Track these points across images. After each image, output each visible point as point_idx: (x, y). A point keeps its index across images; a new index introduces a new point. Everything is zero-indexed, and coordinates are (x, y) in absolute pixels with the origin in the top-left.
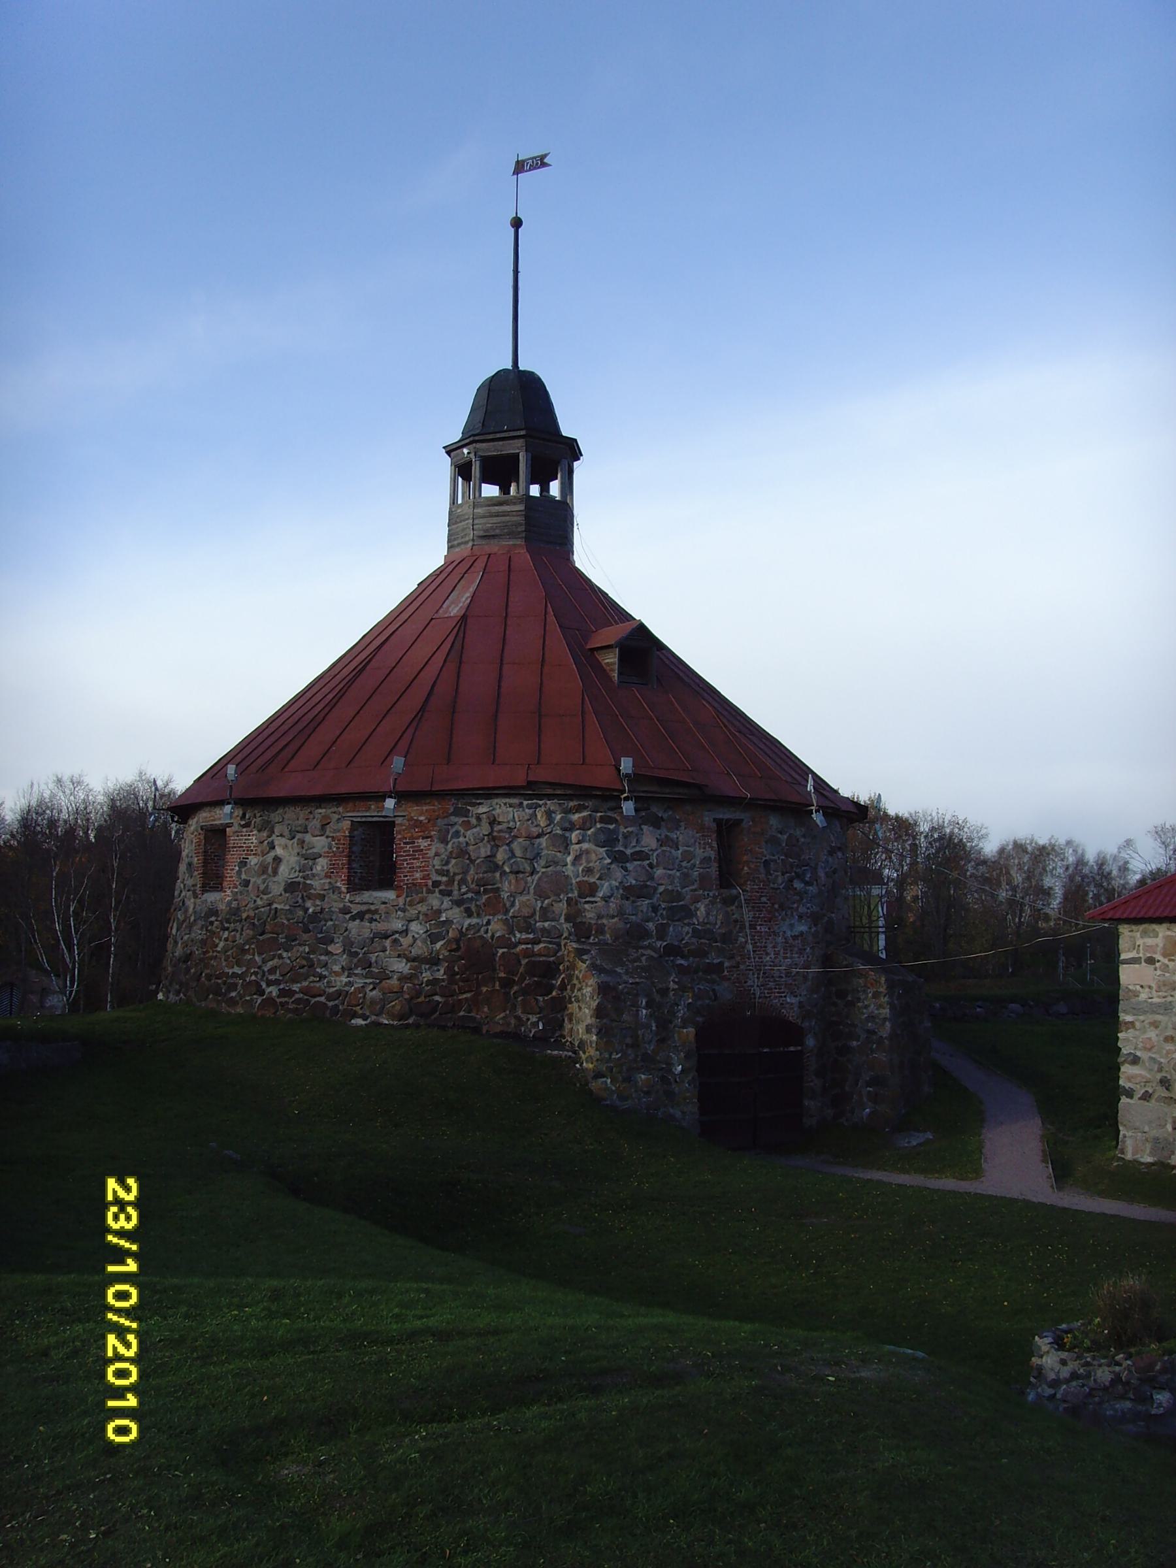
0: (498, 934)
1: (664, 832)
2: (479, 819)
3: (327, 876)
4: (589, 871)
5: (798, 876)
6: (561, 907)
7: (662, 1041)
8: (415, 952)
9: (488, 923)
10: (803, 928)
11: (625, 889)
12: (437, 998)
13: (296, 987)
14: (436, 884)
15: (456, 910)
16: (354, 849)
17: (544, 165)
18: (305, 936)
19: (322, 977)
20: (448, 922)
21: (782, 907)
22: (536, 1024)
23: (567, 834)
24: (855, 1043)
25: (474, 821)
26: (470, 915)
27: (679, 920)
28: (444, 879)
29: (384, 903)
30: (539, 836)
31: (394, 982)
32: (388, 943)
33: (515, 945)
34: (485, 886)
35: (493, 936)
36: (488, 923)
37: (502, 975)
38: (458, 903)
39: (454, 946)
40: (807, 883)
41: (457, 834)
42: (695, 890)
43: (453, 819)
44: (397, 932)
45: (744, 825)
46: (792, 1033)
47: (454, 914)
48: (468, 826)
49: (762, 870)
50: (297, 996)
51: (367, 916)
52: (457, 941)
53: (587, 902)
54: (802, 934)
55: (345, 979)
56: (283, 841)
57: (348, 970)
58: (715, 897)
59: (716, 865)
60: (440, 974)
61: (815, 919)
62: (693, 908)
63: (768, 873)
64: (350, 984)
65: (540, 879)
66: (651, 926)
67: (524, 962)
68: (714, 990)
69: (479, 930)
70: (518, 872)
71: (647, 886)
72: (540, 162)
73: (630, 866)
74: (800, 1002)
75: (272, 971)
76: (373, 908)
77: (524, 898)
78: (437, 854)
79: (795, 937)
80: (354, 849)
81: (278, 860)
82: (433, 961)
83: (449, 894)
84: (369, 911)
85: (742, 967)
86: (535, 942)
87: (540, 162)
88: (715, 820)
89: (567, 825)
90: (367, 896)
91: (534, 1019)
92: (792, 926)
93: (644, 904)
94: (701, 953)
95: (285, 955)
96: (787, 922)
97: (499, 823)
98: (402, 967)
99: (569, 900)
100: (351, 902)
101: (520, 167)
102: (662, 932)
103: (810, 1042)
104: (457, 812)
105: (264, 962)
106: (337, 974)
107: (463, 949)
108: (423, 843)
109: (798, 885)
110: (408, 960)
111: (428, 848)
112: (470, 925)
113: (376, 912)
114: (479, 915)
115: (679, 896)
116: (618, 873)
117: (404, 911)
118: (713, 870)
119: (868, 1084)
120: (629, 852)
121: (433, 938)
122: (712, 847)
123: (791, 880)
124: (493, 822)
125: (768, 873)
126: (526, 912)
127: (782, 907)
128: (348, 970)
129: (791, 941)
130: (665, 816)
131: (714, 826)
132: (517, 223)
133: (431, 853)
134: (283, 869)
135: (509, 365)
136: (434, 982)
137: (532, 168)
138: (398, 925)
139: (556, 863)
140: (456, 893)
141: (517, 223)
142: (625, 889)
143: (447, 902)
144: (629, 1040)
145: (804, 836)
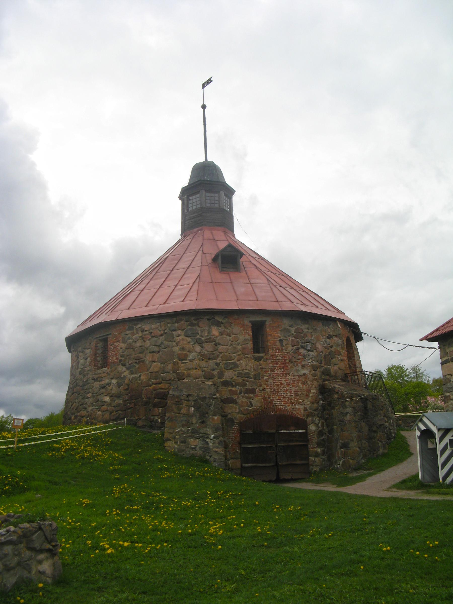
0: (144, 380)
1: (222, 329)
2: (137, 330)
3: (90, 365)
4: (183, 349)
5: (302, 347)
6: (170, 367)
7: (203, 422)
8: (113, 392)
9: (140, 376)
10: (306, 371)
11: (202, 355)
12: (119, 412)
13: (78, 414)
14: (120, 361)
15: (128, 372)
16: (98, 352)
17: (211, 81)
18: (82, 392)
19: (85, 408)
20: (125, 377)
21: (291, 361)
22: (157, 421)
23: (174, 333)
24: (335, 427)
25: (135, 331)
26: (132, 374)
27: (231, 369)
28: (123, 359)
29: (104, 372)
30: (162, 335)
31: (104, 407)
32: (103, 390)
33: (151, 386)
34: (139, 361)
35: (142, 382)
36: (140, 376)
37: (145, 399)
38: (128, 369)
39: (126, 387)
40: (309, 351)
41: (129, 339)
42: (239, 355)
43: (128, 332)
44: (107, 384)
45: (267, 323)
46: (300, 423)
47: (127, 373)
48: (133, 334)
49: (278, 344)
50: (78, 418)
51: (99, 379)
52: (128, 385)
53: (182, 363)
54: (304, 374)
55: (91, 408)
56: (80, 354)
57: (92, 405)
58: (250, 357)
59: (251, 342)
60: (121, 402)
61: (314, 368)
62: (238, 363)
63: (282, 345)
64: (92, 410)
65: (162, 354)
66: (215, 373)
67: (154, 392)
68: (250, 402)
69: (136, 380)
70: (153, 352)
71: (213, 354)
72: (210, 81)
73: (203, 344)
74: (304, 408)
75: (73, 409)
76: (100, 375)
77: (155, 364)
78: (121, 348)
79: (299, 376)
80: (98, 352)
81: (79, 362)
82: (118, 397)
83: (124, 365)
84: (98, 377)
85: (267, 390)
86: (159, 384)
87: (210, 81)
88: (250, 322)
89: (173, 328)
90: (99, 371)
91: (156, 418)
92: (297, 371)
93: (212, 363)
94: (244, 385)
95: (77, 401)
96: (294, 369)
97: (146, 331)
98: (107, 399)
99: (174, 364)
100: (95, 374)
101: (204, 85)
102: (221, 375)
103: (312, 428)
104: (130, 329)
105: (72, 405)
106: (89, 406)
107: (130, 389)
108: (116, 344)
109: (302, 351)
110: (111, 397)
111: (118, 346)
112: (133, 377)
113: (101, 377)
114: (136, 374)
115: (231, 358)
116: (198, 348)
117: (109, 375)
118: (250, 345)
119: (341, 448)
120: (203, 339)
121: (119, 385)
122: (249, 334)
123: (298, 349)
124: (143, 331)
125: (282, 345)
126: (156, 370)
127: (291, 361)
128: (92, 405)
129: (297, 378)
130: (224, 321)
131: (250, 324)
132: (204, 107)
133: (119, 348)
134: (80, 365)
135: (203, 160)
136: (119, 405)
137: (208, 84)
138: (107, 381)
139: (169, 346)
140: (128, 364)
141: (204, 107)
142: (202, 355)
143: (124, 369)
144: (184, 422)
145: (308, 329)
